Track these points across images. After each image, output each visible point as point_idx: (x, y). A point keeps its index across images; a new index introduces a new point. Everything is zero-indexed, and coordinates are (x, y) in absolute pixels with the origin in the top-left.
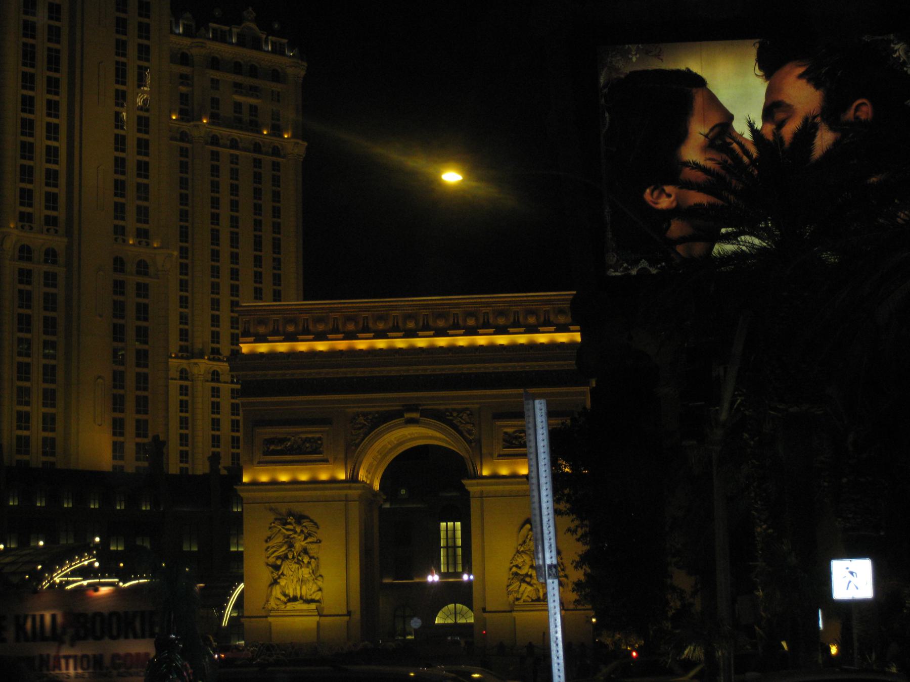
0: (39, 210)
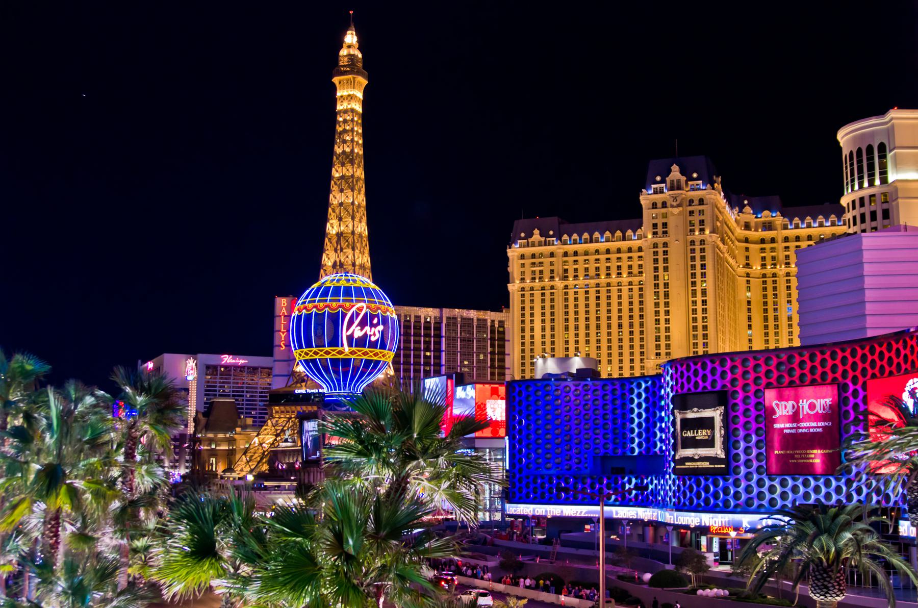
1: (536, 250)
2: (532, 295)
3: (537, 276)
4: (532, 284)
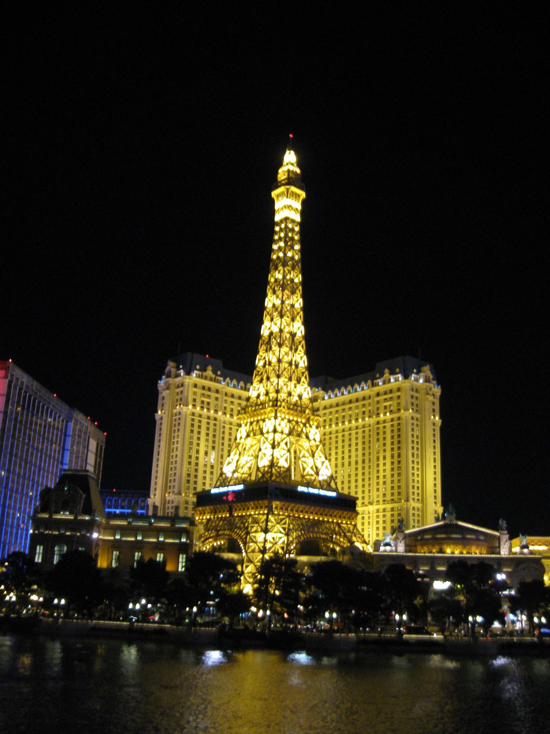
0: (416, 497)
1: (207, 383)
2: (200, 421)
3: (205, 405)
4: (201, 412)
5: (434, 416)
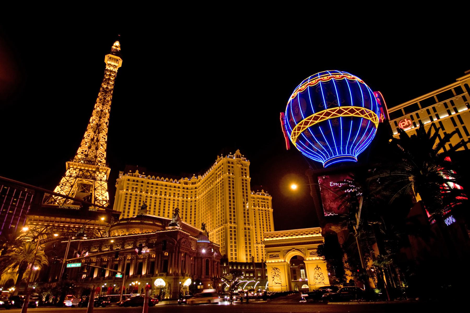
0: (233, 221)
1: (136, 178)
2: (131, 197)
3: (135, 189)
4: (131, 193)
5: (246, 176)
